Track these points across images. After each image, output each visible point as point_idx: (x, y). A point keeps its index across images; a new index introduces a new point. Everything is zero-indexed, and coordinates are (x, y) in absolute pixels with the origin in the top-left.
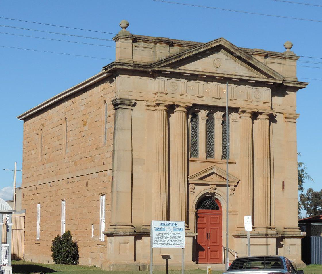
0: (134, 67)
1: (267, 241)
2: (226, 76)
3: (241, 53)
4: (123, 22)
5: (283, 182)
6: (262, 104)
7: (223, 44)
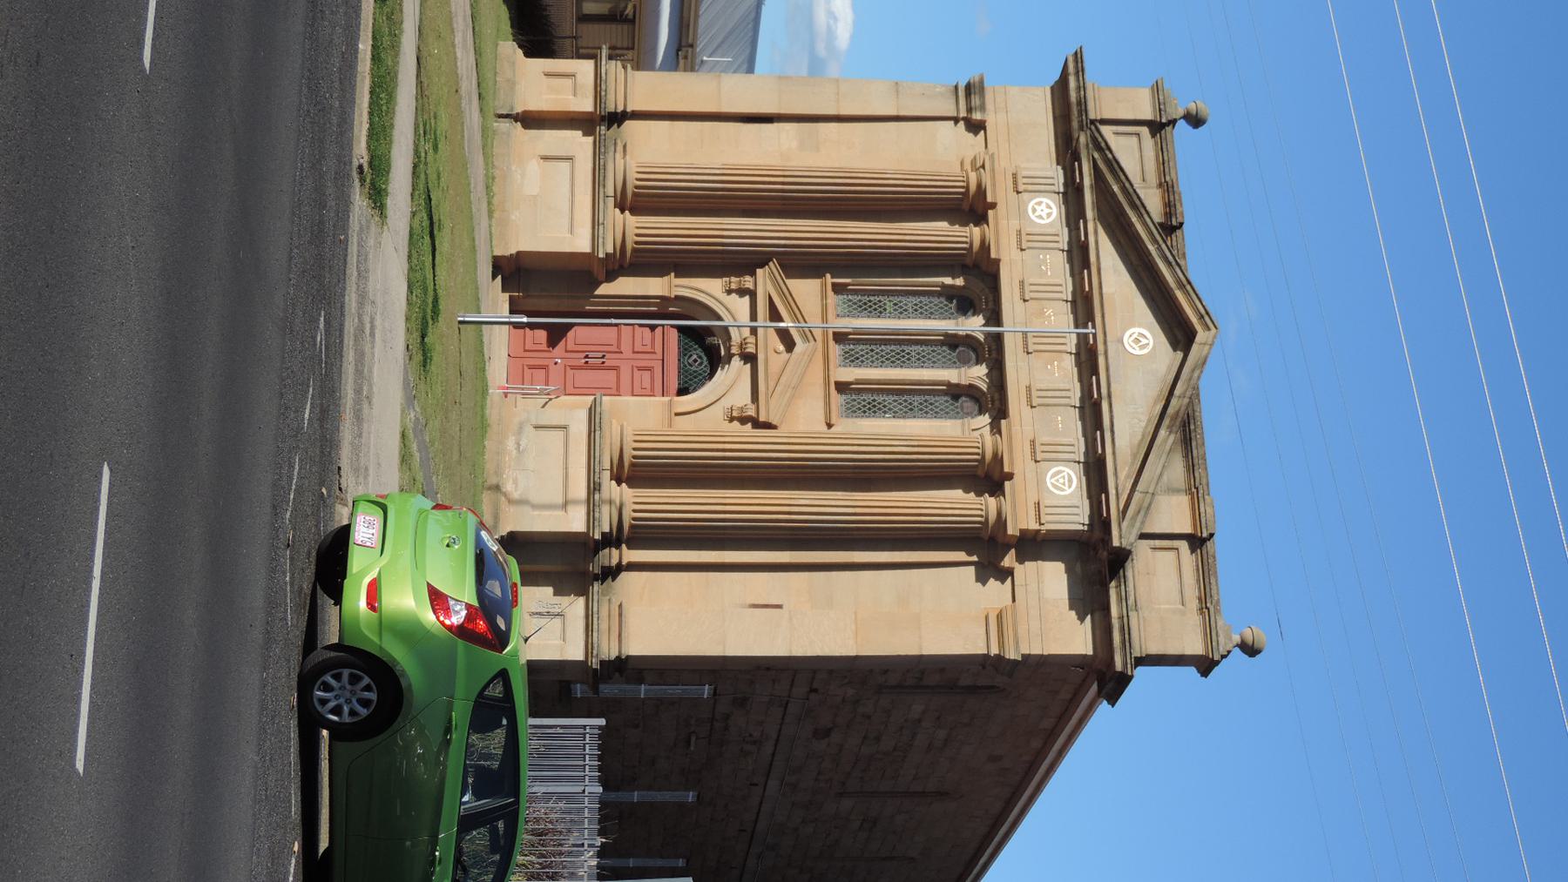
0: (1079, 103)
1: (576, 502)
2: (1100, 348)
3: (1182, 396)
4: (1204, 108)
5: (780, 607)
6: (1032, 499)
7: (1198, 339)
